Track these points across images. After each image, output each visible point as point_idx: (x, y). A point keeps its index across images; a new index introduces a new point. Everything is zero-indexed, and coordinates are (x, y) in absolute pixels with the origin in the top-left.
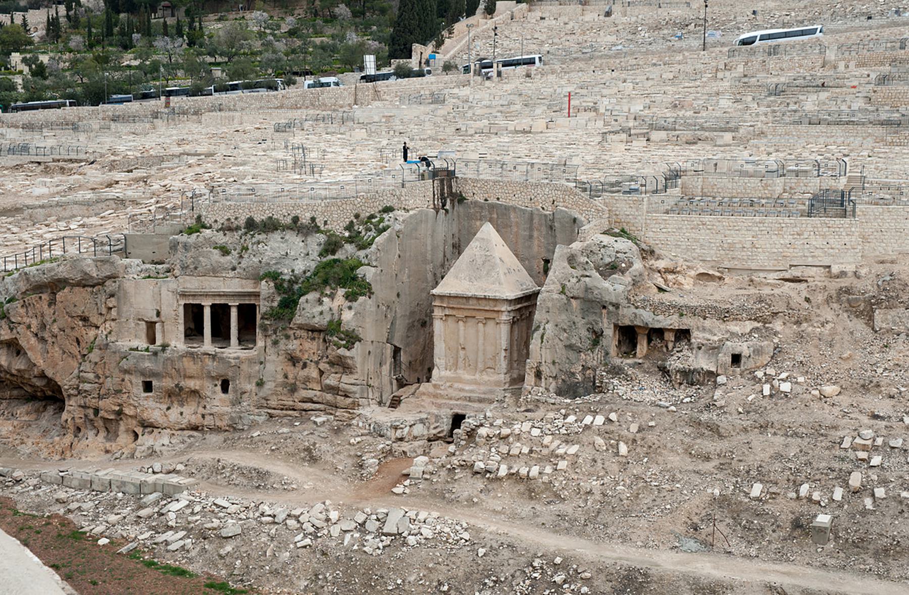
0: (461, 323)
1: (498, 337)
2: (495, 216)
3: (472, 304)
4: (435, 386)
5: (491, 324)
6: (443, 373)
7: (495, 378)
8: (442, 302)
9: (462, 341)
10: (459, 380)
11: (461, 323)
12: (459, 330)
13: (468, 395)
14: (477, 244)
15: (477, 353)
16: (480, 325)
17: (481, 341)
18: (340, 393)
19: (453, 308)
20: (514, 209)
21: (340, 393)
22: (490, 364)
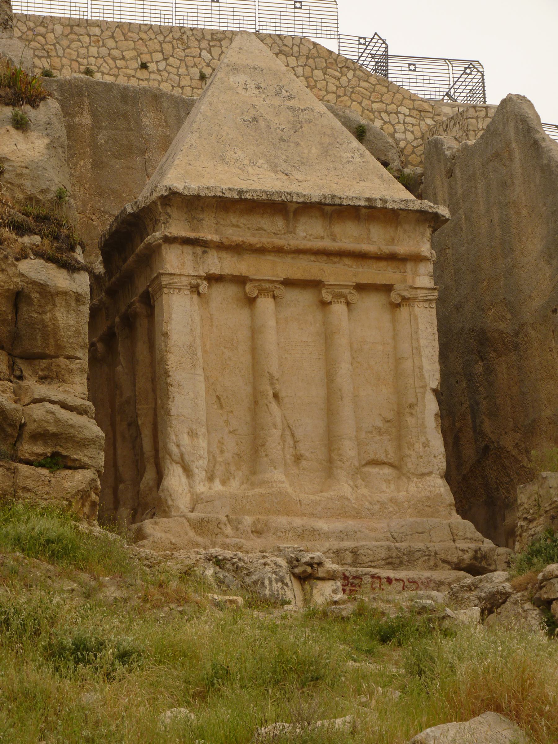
0: (266, 304)
1: (405, 347)
2: (86, 120)
3: (310, 232)
4: (200, 526)
5: (372, 306)
6: (201, 488)
7: (413, 489)
8: (193, 230)
9: (273, 365)
10: (286, 506)
11: (266, 304)
12: (255, 332)
13: (349, 544)
14: (241, 78)
15: (330, 412)
16: (339, 308)
17: (344, 367)
18: (28, 449)
19: (238, 249)
20: (156, 97)
21: (28, 449)
22: (381, 447)
